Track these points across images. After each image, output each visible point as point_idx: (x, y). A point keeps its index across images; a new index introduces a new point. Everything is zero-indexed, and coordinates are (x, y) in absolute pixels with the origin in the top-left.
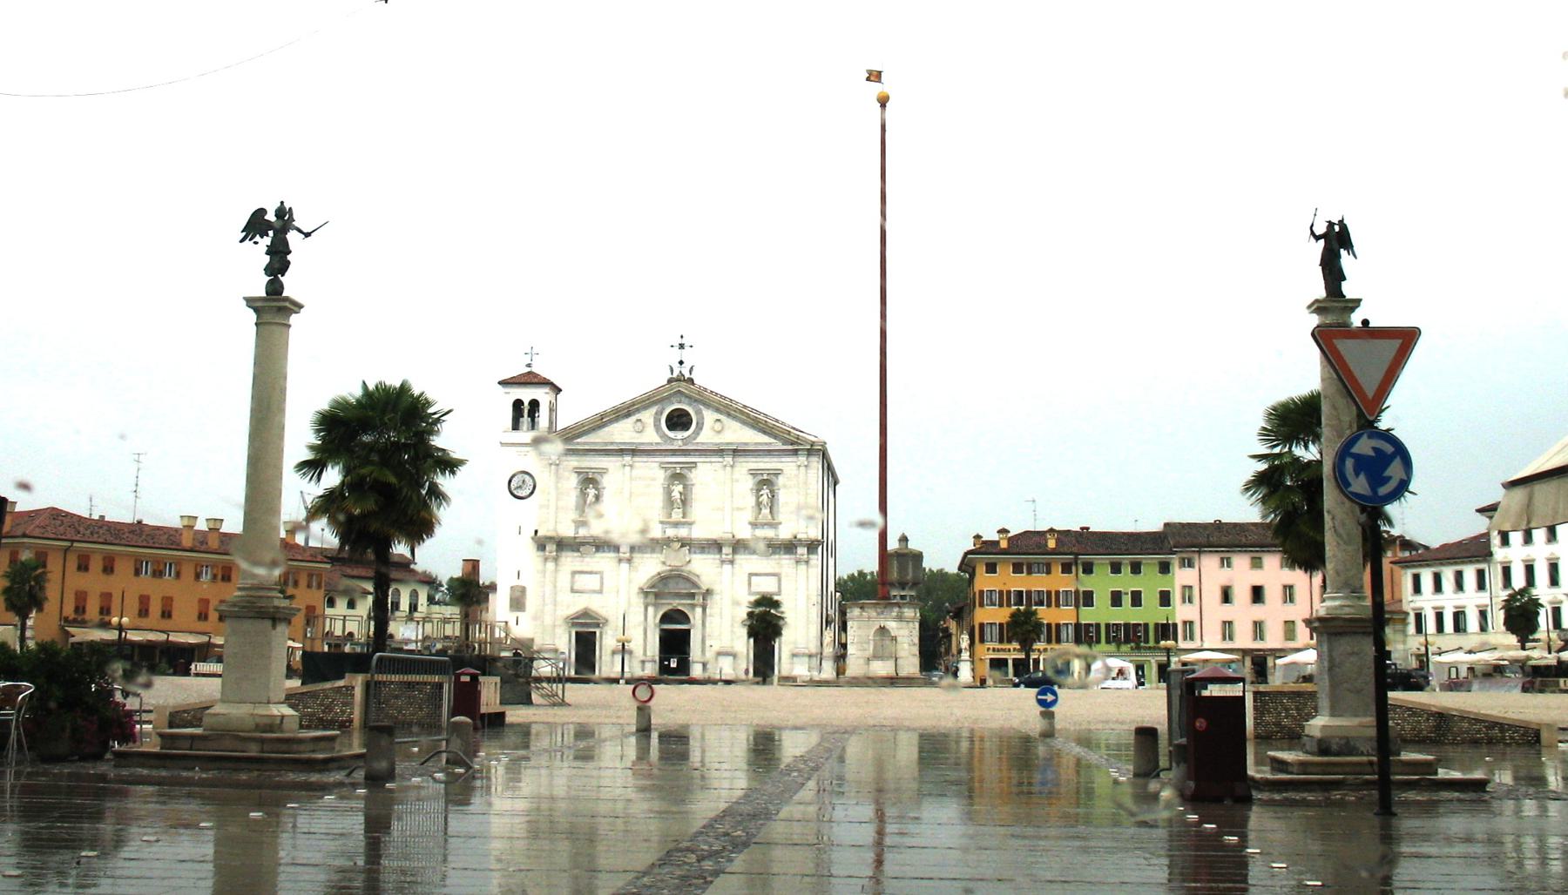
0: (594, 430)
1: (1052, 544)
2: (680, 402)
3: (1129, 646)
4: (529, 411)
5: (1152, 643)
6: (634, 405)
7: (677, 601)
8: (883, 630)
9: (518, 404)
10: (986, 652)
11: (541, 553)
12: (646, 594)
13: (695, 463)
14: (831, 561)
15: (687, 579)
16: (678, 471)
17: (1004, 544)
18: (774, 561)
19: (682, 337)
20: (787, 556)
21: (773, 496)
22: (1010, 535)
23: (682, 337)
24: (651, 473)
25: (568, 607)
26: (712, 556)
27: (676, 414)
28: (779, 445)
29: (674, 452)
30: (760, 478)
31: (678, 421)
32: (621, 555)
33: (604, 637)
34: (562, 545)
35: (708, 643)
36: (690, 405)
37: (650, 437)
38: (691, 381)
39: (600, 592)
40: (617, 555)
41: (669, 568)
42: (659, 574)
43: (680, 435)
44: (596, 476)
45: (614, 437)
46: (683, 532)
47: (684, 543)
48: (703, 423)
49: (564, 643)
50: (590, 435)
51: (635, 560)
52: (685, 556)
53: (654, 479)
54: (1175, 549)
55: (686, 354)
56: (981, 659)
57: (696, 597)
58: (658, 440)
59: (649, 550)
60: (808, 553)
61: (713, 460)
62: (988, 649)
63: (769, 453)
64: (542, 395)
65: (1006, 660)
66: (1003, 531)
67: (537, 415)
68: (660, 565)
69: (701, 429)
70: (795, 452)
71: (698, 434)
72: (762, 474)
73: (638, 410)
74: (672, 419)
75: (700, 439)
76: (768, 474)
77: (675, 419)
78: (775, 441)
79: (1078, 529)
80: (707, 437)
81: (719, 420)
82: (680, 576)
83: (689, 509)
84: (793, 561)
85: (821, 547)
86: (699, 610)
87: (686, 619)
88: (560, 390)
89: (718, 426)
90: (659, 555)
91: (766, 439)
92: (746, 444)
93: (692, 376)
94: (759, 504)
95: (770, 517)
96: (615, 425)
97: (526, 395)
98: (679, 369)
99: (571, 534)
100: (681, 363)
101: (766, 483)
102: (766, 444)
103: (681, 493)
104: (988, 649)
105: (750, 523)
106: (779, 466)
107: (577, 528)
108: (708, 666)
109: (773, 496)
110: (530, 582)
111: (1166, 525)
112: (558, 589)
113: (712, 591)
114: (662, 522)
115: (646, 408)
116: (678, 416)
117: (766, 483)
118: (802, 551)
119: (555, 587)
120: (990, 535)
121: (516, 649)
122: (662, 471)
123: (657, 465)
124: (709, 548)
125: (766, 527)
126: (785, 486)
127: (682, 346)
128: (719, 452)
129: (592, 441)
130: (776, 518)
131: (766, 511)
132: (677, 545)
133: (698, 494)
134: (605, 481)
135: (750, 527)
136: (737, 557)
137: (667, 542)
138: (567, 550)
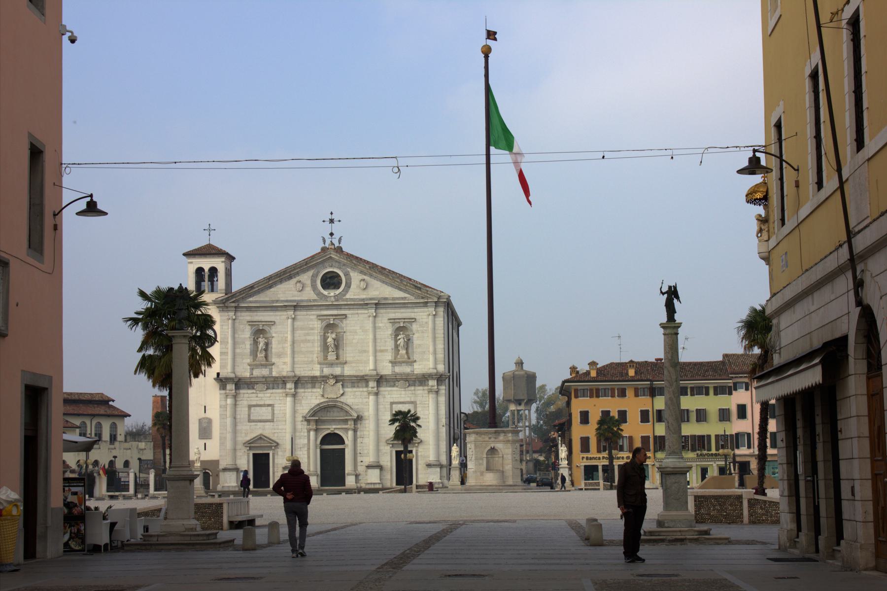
0: (262, 290)
1: (631, 372)
3: (695, 453)
4: (209, 276)
5: (713, 451)
6: (295, 269)
7: (334, 427)
8: (493, 450)
9: (199, 271)
10: (581, 461)
11: (223, 392)
12: (308, 421)
13: (346, 315)
14: (456, 390)
15: (342, 409)
16: (332, 322)
17: (593, 374)
18: (410, 392)
19: (332, 213)
20: (421, 388)
21: (408, 341)
22: (598, 366)
23: (332, 213)
24: (312, 323)
25: (246, 434)
26: (361, 389)
27: (329, 276)
28: (412, 299)
29: (328, 307)
30: (397, 325)
31: (331, 281)
32: (287, 390)
33: (276, 457)
34: (240, 383)
35: (359, 459)
36: (340, 268)
37: (309, 294)
38: (339, 250)
39: (272, 421)
40: (284, 391)
41: (326, 400)
42: (318, 405)
43: (332, 293)
44: (266, 328)
45: (279, 296)
46: (337, 371)
47: (338, 379)
48: (351, 283)
49: (245, 462)
50: (260, 295)
51: (299, 395)
52: (339, 390)
53: (312, 329)
54: (730, 376)
55: (336, 228)
56: (577, 466)
57: (349, 423)
58: (315, 297)
59: (310, 385)
60: (438, 385)
61: (360, 311)
62: (583, 458)
63: (405, 305)
64: (219, 263)
65: (597, 466)
66: (593, 364)
67: (215, 279)
68: (320, 397)
69: (349, 287)
70: (426, 304)
71: (347, 292)
72: (399, 322)
73: (298, 274)
74: (327, 278)
75: (348, 296)
76: (404, 322)
77: (328, 280)
78: (410, 296)
79: (654, 361)
80: (355, 293)
81: (364, 280)
82: (335, 406)
83: (341, 352)
84: (426, 392)
85: (447, 380)
86: (350, 433)
87: (341, 441)
88: (234, 258)
89: (363, 285)
90: (319, 390)
91: (401, 294)
92: (386, 299)
93: (340, 245)
94: (397, 346)
95: (406, 356)
96: (279, 286)
97: (206, 264)
98: (330, 240)
99: (247, 375)
100: (332, 234)
101: (401, 329)
103: (334, 340)
104: (583, 458)
105: (391, 362)
106: (413, 315)
107: (252, 369)
108: (360, 477)
109: (409, 340)
110: (214, 414)
111: (726, 356)
112: (238, 420)
113: (362, 417)
114: (320, 364)
115: (304, 271)
116: (330, 278)
117: (401, 329)
118: (432, 383)
119: (235, 418)
120: (583, 367)
121: (205, 469)
122: (320, 322)
123: (315, 317)
124: (358, 382)
125: (403, 364)
126: (418, 331)
127: (332, 221)
128: (363, 305)
129: (261, 299)
130: (411, 358)
131: (403, 352)
132: (332, 381)
133: (348, 338)
134: (274, 332)
135: (390, 365)
136: (382, 389)
137: (324, 379)
138: (244, 388)
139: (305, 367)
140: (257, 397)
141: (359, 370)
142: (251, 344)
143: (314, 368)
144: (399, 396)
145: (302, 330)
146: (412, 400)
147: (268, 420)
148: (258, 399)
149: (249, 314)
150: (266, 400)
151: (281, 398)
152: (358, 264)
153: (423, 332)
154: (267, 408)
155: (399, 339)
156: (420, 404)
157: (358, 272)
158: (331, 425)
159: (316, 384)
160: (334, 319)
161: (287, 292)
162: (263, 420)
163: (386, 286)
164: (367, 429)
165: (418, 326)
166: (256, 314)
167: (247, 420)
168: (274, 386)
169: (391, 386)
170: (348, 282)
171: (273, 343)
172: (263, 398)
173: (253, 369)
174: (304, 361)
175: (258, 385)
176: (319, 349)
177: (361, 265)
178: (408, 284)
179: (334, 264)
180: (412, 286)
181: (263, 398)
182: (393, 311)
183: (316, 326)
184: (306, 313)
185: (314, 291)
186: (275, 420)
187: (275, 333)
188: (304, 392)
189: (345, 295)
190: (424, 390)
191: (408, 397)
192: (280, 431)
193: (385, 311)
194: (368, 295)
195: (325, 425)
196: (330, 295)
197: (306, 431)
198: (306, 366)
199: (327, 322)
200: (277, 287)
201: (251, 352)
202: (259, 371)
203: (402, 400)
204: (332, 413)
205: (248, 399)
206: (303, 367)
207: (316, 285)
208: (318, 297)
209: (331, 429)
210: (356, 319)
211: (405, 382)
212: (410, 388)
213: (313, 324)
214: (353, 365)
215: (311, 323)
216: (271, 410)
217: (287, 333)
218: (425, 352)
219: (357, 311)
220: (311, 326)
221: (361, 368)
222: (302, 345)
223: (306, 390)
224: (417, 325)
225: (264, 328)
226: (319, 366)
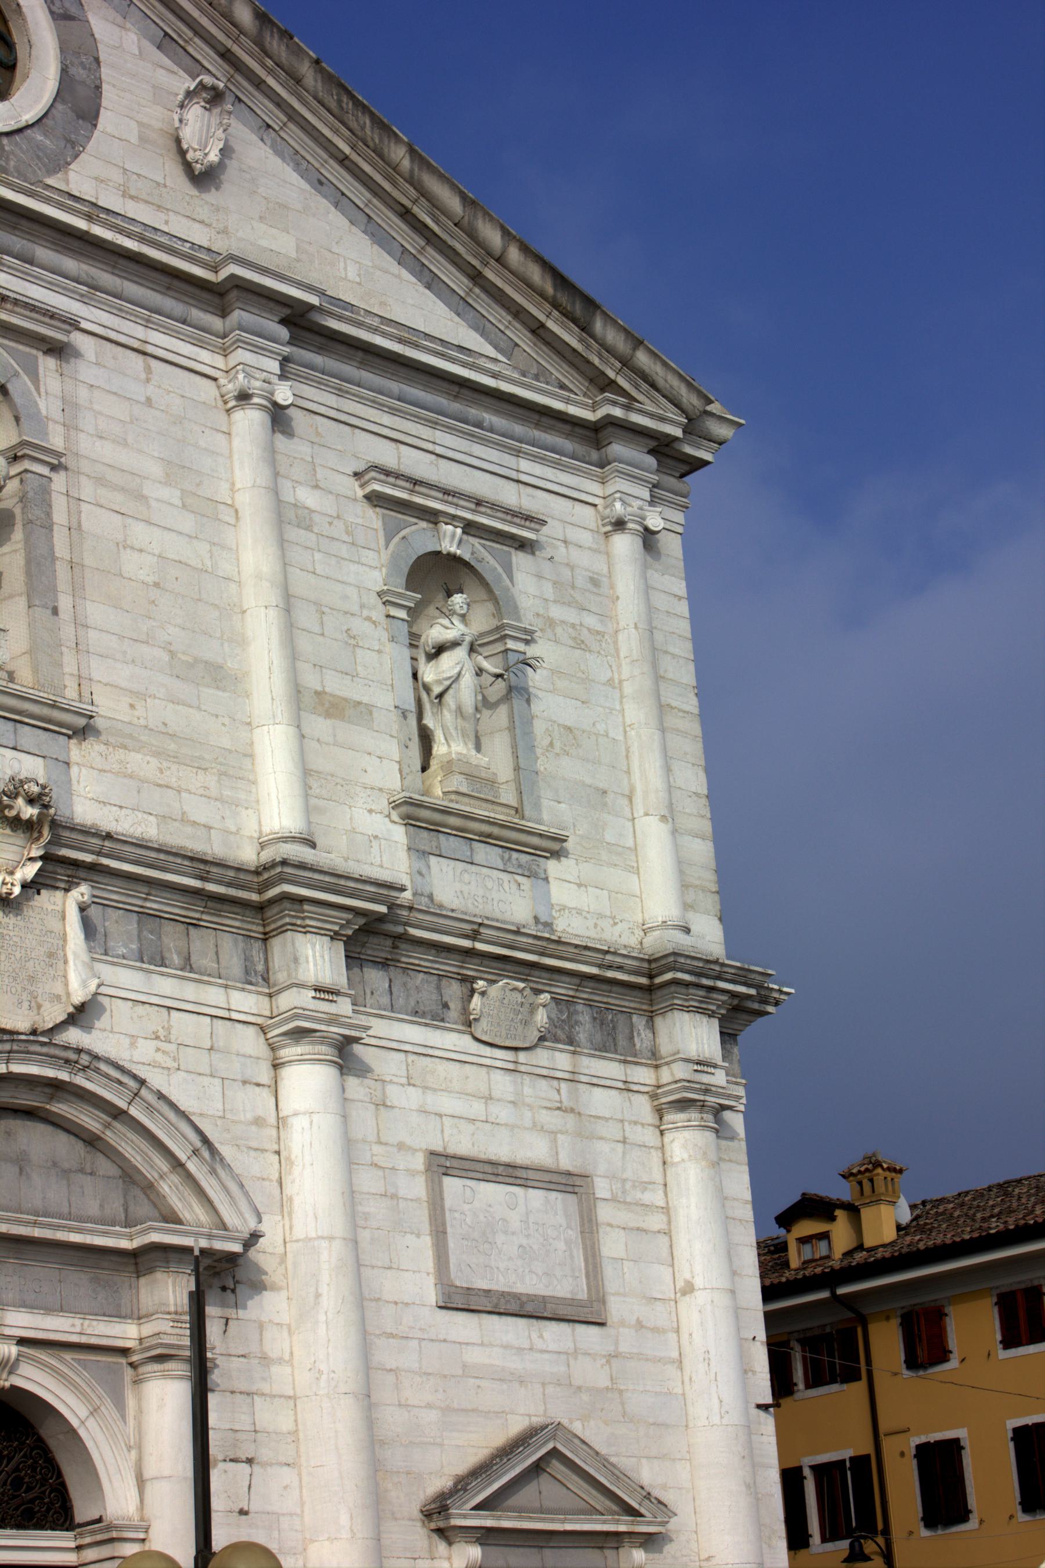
20: (609, 1069)
26: (213, 996)
48: (98, 88)
52: (56, 957)
72: (432, 517)
76: (470, 528)
78: (491, 352)
102: (444, 347)
135: (399, 834)
141: (184, 820)
144: (477, 1109)
146: (565, 1163)
153: (580, 645)
155: (440, 650)
156: (614, 1199)
157: (145, 34)
163: (337, 219)
164: (281, 1378)
165: (549, 591)
169: (419, 1014)
170: (78, 73)
178: (514, 255)
180: (535, 274)
182: (386, 419)
189: (60, 165)
190: (627, 1088)
191: (538, 1128)
193: (332, 400)
194: (224, 231)
203: (501, 1149)
210: (139, 391)
211: (532, 998)
212: (542, 1057)
214: (141, 763)
218: (605, 792)
219: (140, 332)
221: (201, 811)
224: (539, 577)
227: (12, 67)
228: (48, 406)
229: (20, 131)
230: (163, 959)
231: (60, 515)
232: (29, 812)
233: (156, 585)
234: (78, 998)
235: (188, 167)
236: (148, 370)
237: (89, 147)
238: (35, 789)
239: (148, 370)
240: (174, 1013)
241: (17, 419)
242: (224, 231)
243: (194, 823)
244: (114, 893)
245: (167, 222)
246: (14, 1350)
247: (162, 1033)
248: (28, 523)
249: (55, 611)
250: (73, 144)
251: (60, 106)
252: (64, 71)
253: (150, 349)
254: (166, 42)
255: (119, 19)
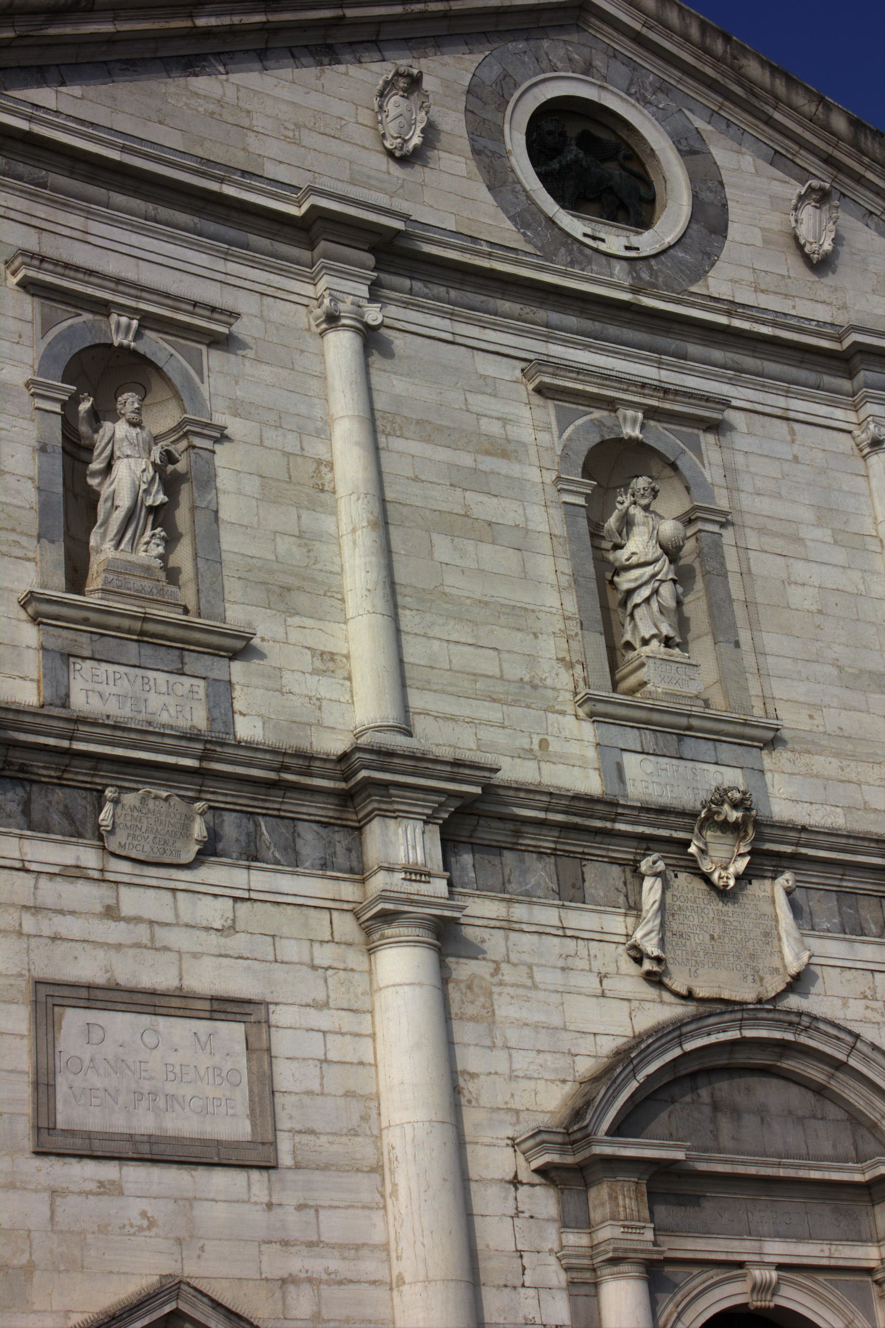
2: (588, 69)
40: (348, 891)
48: (725, 206)
52: (771, 935)
71: (710, 257)
122: (549, 411)
139: (490, 724)
140: (111, 913)
141: (867, 808)
142: (43, 449)
143: (555, 746)
145: (427, 439)
147: (205, 1143)
148: (115, 932)
149: (22, 204)
150: (195, 956)
151: (324, 955)
152: (780, 87)
154: (203, 1027)
157: (758, 155)
158: (749, 1233)
159: (591, 871)
160: (651, 413)
161: (310, 139)
162: (178, 1141)
166: (76, 220)
167: (23, 1127)
168: (253, 837)
171: (224, 479)
172: (166, 936)
173: (67, 657)
174: (475, 676)
175: (129, 799)
176: (571, 606)
177: (800, 100)
179: (598, 63)
181: (166, 936)
183: (526, 434)
184: (445, 324)
185: (490, 189)
186: (286, 1159)
187: (236, 409)
188: (508, 926)
189: (699, 274)
192: (334, 1264)
194: (844, 307)
195: (706, 1232)
196: (602, 247)
197: (557, 1276)
198: (492, 712)
199: (599, 424)
200: (235, 78)
201: (44, 510)
202: (124, 686)
204: (750, 1121)
205: (29, 924)
206: (471, 722)
207: (503, 155)
208: (528, 241)
209: (758, 1274)
210: (785, 451)
213: (504, 421)
214: (823, 764)
215: (494, 406)
216: (240, 1047)
217: (324, 432)
219: (781, 402)
220: (494, 428)
222: (443, 548)
223: (519, 912)
225: (141, 347)
226: (588, 731)
227: (652, 201)
228: (712, 474)
229: (663, 252)
230: (862, 929)
231: (732, 564)
232: (734, 815)
233: (820, 612)
234: (794, 967)
235: (806, 258)
236: (792, 432)
237: (722, 256)
238: (738, 796)
239: (792, 432)
240: (877, 975)
241: (688, 489)
242: (844, 307)
243: (876, 810)
244: (814, 877)
245: (794, 307)
246: (774, 1275)
247: (869, 993)
248: (706, 574)
249: (737, 644)
250: (709, 255)
251: (695, 226)
252: (695, 197)
253: (792, 415)
254: (777, 159)
255: (736, 146)
